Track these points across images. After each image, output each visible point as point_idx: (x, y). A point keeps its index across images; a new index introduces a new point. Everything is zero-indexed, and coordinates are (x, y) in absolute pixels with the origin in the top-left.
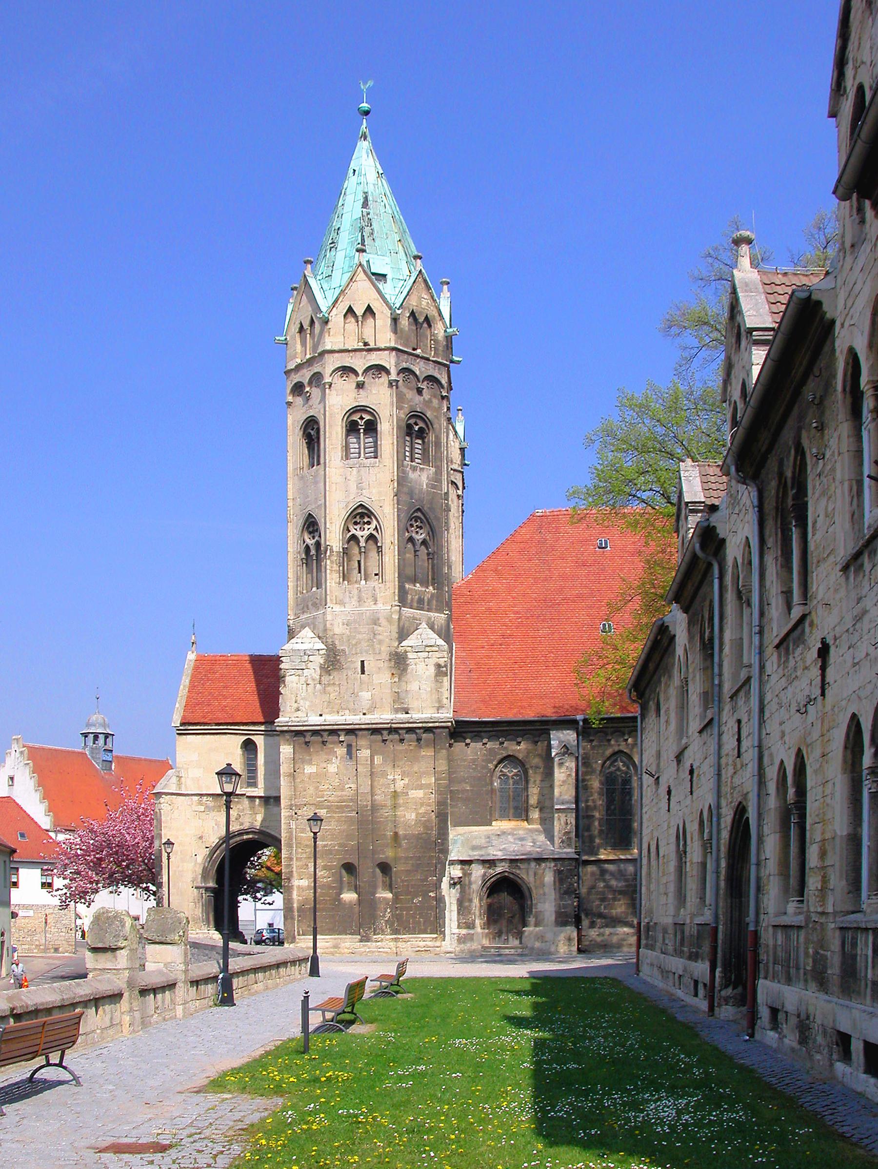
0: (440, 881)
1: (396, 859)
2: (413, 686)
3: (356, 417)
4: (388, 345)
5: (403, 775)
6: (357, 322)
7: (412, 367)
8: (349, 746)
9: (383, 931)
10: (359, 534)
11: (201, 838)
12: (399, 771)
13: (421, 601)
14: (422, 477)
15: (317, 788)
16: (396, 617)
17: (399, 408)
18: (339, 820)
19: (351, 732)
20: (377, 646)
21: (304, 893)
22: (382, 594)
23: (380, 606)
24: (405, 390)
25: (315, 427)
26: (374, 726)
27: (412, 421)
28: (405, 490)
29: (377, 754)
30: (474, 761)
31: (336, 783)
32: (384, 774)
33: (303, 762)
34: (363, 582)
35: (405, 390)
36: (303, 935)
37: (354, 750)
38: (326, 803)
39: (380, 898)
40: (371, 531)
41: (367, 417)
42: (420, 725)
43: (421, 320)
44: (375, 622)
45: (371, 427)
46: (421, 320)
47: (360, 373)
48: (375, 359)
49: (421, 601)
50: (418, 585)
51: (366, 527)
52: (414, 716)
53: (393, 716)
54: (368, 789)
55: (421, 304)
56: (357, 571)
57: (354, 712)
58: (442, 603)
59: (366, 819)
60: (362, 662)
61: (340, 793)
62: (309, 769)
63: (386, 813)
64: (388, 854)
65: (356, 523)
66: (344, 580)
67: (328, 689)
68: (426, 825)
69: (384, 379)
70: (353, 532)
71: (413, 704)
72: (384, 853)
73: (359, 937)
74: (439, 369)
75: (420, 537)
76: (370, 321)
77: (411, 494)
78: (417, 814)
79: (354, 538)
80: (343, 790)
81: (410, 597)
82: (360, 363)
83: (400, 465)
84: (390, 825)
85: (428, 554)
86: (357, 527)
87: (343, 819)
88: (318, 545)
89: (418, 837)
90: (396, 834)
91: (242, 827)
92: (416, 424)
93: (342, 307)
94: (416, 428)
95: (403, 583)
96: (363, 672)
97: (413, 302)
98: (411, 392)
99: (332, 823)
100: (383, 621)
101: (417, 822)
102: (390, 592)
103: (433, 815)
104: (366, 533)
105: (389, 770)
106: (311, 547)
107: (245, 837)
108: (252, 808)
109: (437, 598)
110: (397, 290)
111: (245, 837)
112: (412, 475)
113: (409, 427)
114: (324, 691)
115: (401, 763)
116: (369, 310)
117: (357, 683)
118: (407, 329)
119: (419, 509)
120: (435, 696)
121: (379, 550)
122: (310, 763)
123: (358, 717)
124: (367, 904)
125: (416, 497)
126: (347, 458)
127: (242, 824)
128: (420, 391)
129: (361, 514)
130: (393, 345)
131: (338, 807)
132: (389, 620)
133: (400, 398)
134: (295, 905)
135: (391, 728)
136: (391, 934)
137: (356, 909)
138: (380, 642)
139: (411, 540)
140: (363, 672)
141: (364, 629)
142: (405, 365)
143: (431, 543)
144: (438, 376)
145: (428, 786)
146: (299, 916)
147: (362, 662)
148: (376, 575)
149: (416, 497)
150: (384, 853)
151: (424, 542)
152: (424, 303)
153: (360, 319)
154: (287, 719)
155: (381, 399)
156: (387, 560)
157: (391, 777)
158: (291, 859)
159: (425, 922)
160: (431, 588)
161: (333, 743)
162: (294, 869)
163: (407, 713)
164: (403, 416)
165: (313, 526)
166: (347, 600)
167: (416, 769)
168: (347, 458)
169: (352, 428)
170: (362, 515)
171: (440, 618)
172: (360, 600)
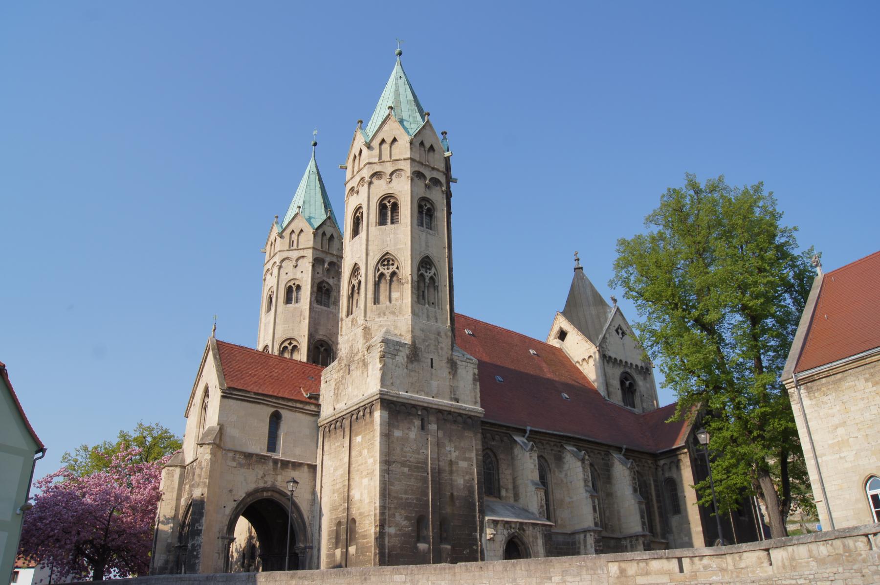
5: (456, 448)
8: (422, 420)
15: (402, 449)
20: (440, 351)
37: (426, 423)
44: (439, 334)
57: (427, 394)
62: (397, 433)
63: (445, 476)
64: (448, 510)
80: (419, 454)
96: (432, 367)
99: (413, 480)
100: (442, 334)
105: (447, 442)
138: (442, 348)
140: (432, 367)
141: (433, 336)
157: (448, 449)
167: (462, 445)
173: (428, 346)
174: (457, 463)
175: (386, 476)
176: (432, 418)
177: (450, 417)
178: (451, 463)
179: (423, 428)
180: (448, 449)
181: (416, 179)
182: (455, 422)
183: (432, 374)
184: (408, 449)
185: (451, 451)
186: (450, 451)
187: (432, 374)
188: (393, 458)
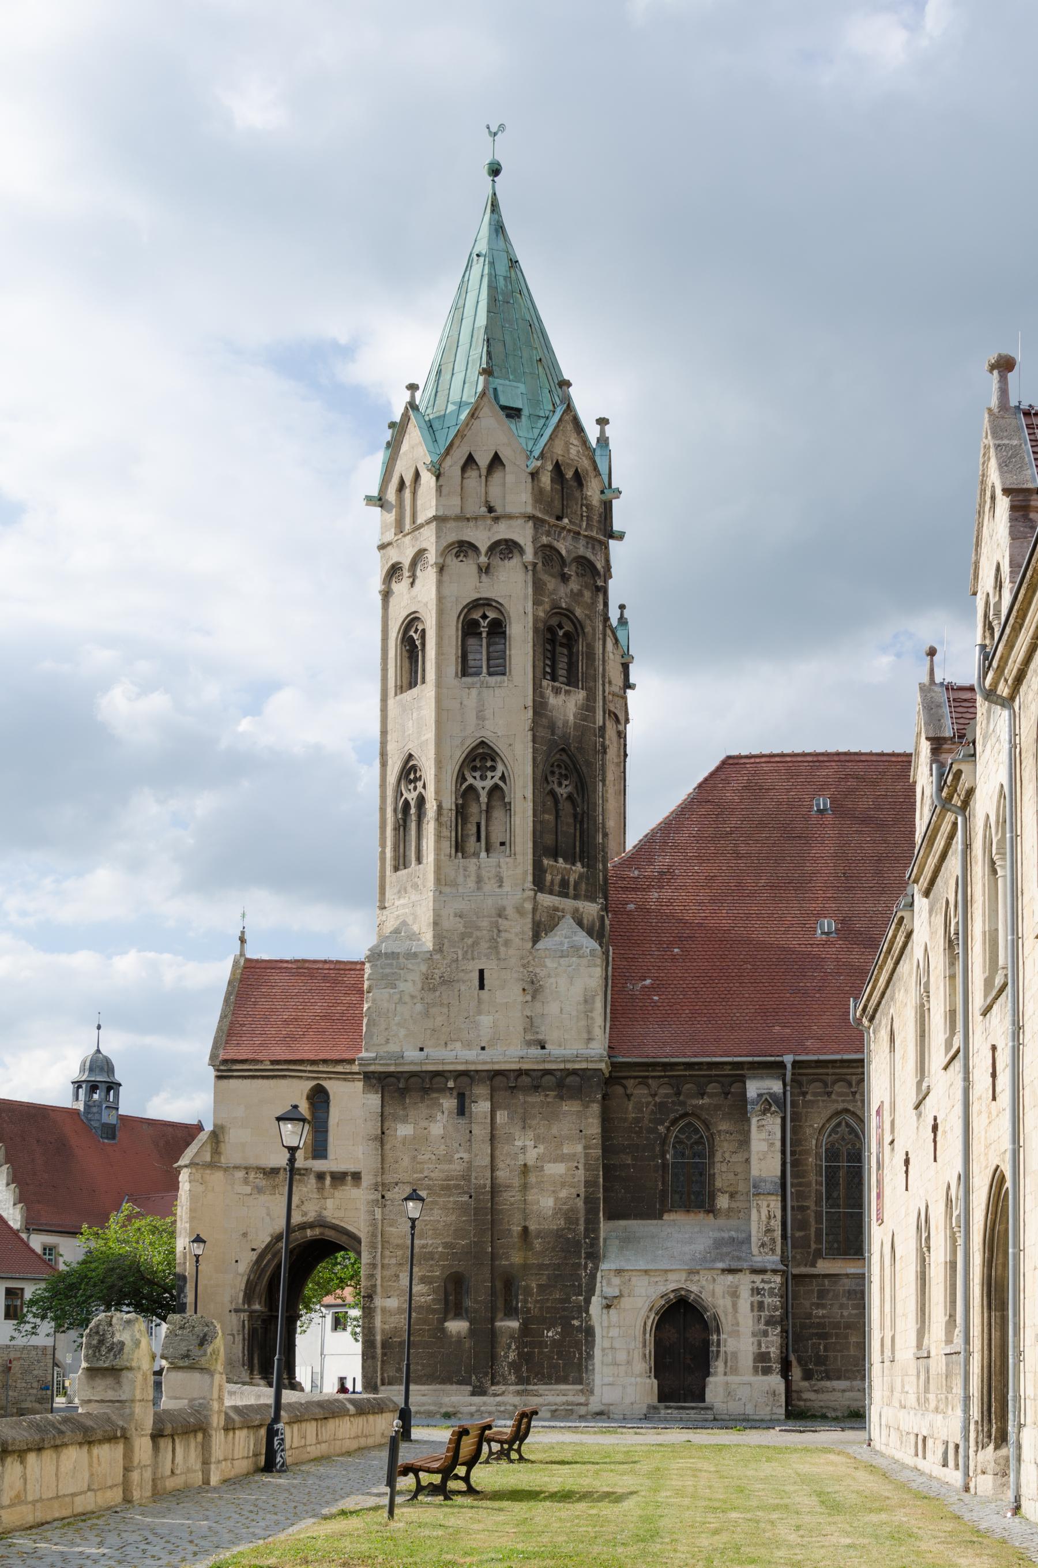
0: (588, 1301)
1: (525, 1266)
2: (553, 1008)
3: (476, 615)
4: (523, 511)
5: (538, 1140)
6: (480, 476)
7: (555, 544)
8: (461, 1098)
9: (505, 1378)
10: (478, 784)
11: (245, 1235)
12: (531, 1134)
13: (564, 883)
14: (567, 706)
16: (529, 906)
17: (536, 603)
18: (444, 1208)
20: (502, 949)
21: (392, 1319)
22: (510, 872)
23: (507, 887)
24: (545, 577)
25: (420, 628)
26: (497, 1067)
27: (554, 622)
28: (545, 721)
29: (500, 1108)
30: (638, 1120)
31: (442, 1150)
32: (510, 1139)
33: (395, 1118)
34: (483, 854)
35: (545, 577)
36: (390, 1384)
37: (467, 1101)
38: (427, 1182)
39: (501, 1327)
40: (496, 780)
41: (492, 615)
42: (562, 1066)
43: (569, 474)
44: (501, 914)
45: (498, 629)
46: (569, 474)
47: (483, 549)
48: (503, 531)
49: (564, 883)
50: (561, 860)
51: (489, 774)
52: (554, 1052)
55: (569, 453)
56: (473, 839)
57: (468, 1045)
58: (596, 886)
59: (486, 1208)
60: (481, 972)
61: (446, 1167)
62: (404, 1130)
63: (510, 1197)
65: (474, 769)
66: (457, 851)
67: (433, 1011)
68: (570, 1218)
69: (515, 562)
70: (470, 781)
71: (551, 1034)
72: (507, 1259)
73: (470, 1388)
74: (593, 548)
75: (562, 791)
76: (497, 476)
77: (552, 727)
78: (557, 1199)
79: (471, 787)
80: (451, 1162)
81: (549, 877)
82: (482, 537)
83: (537, 687)
84: (517, 1217)
85: (575, 816)
86: (477, 774)
87: (450, 1206)
88: (421, 800)
89: (558, 1234)
90: (525, 1229)
91: (305, 1219)
92: (561, 627)
93: (459, 456)
94: (561, 633)
95: (540, 856)
96: (482, 986)
97: (558, 450)
98: (553, 580)
99: (436, 1212)
100: (510, 911)
101: (557, 1211)
102: (519, 871)
103: (580, 1203)
104: (488, 783)
106: (412, 804)
107: (309, 1233)
108: (321, 1189)
109: (588, 879)
110: (536, 432)
111: (309, 1233)
112: (553, 700)
113: (550, 630)
114: (427, 1014)
115: (534, 1122)
116: (496, 461)
118: (549, 488)
119: (563, 750)
120: (583, 1023)
121: (507, 807)
122: (405, 1120)
123: (474, 1052)
124: (485, 1337)
125: (559, 732)
126: (464, 673)
127: (305, 1214)
128: (564, 578)
129: (481, 757)
130: (529, 510)
131: (444, 1188)
132: (520, 911)
133: (538, 587)
134: (379, 1338)
135: (520, 1070)
136: (517, 1384)
137: (468, 1344)
138: (507, 943)
139: (552, 793)
140: (482, 986)
141: (485, 924)
142: (545, 540)
143: (579, 800)
144: (592, 558)
145: (572, 1157)
146: (384, 1354)
147: (481, 972)
148: (502, 844)
149: (559, 732)
150: (507, 1259)
151: (570, 797)
152: (573, 451)
153: (484, 472)
154: (373, 1055)
155: (513, 589)
156: (518, 822)
157: (519, 1143)
158: (374, 1266)
159: (565, 1365)
160: (579, 864)
162: (379, 1282)
163: (543, 1048)
164: (542, 614)
165: (415, 773)
166: (461, 879)
168: (464, 673)
169: (469, 629)
170: (484, 757)
171: (591, 909)
172: (479, 880)
174: (541, 1169)
175: (378, 1213)
176: (481, 1091)
177: (525, 1080)
178: (525, 1169)
179: (462, 1110)
180: (519, 1143)
181: (452, 562)
182: (536, 1088)
183: (480, 1001)
184: (426, 1157)
185: (525, 1146)
186: (524, 1148)
187: (480, 1001)
188: (389, 1178)
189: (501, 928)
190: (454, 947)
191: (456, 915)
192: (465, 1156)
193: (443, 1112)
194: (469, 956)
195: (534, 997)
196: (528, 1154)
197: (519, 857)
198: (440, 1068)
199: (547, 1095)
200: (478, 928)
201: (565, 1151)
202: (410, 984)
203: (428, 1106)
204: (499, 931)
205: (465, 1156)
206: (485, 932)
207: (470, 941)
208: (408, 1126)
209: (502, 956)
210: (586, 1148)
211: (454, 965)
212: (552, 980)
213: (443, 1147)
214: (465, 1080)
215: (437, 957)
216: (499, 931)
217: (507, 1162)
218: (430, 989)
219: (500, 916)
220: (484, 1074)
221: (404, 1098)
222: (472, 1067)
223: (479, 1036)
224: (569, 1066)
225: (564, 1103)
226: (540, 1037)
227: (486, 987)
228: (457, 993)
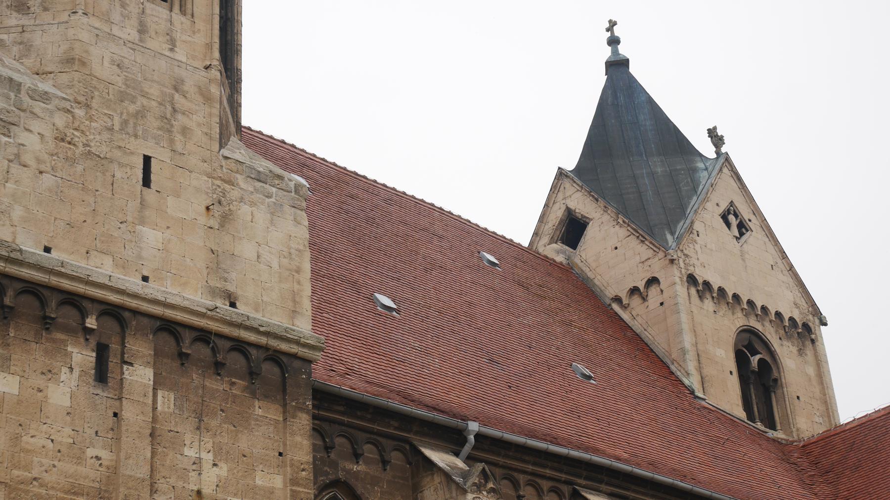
5: (220, 454)
8: (102, 351)
19: (115, 313)
20: (178, 137)
26: (169, 313)
31: (65, 436)
32: (178, 444)
37: (113, 361)
42: (263, 340)
53: (210, 303)
54: (143, 472)
60: (147, 160)
61: (70, 467)
80: (79, 460)
96: (147, 182)
102: (200, 39)
115: (214, 423)
117: (133, 205)
138: (185, 131)
140: (147, 182)
141: (154, 91)
147: (147, 160)
157: (190, 453)
161: (67, 329)
173: (140, 114)
176: (140, 346)
179: (101, 375)
180: (190, 453)
183: (143, 203)
186: (198, 462)
187: (143, 203)
189: (177, 106)
190: (108, 107)
191: (113, 62)
192: (104, 454)
193: (71, 369)
194: (130, 129)
195: (222, 225)
196: (204, 476)
197: (200, 25)
198: (81, 288)
199: (233, 384)
200: (145, 95)
201: (259, 482)
202: (35, 138)
203: (46, 352)
204: (175, 110)
205: (104, 454)
206: (154, 104)
207: (132, 108)
208: (10, 377)
209: (179, 147)
210: (294, 482)
211: (106, 136)
212: (245, 209)
213: (68, 430)
214: (111, 324)
215: (80, 112)
216: (175, 110)
217: (172, 481)
218: (67, 159)
219: (176, 89)
220: (145, 321)
221: (7, 326)
222: (133, 303)
223: (140, 257)
224: (274, 343)
225: (257, 403)
226: (231, 288)
227: (152, 185)
228: (110, 179)
